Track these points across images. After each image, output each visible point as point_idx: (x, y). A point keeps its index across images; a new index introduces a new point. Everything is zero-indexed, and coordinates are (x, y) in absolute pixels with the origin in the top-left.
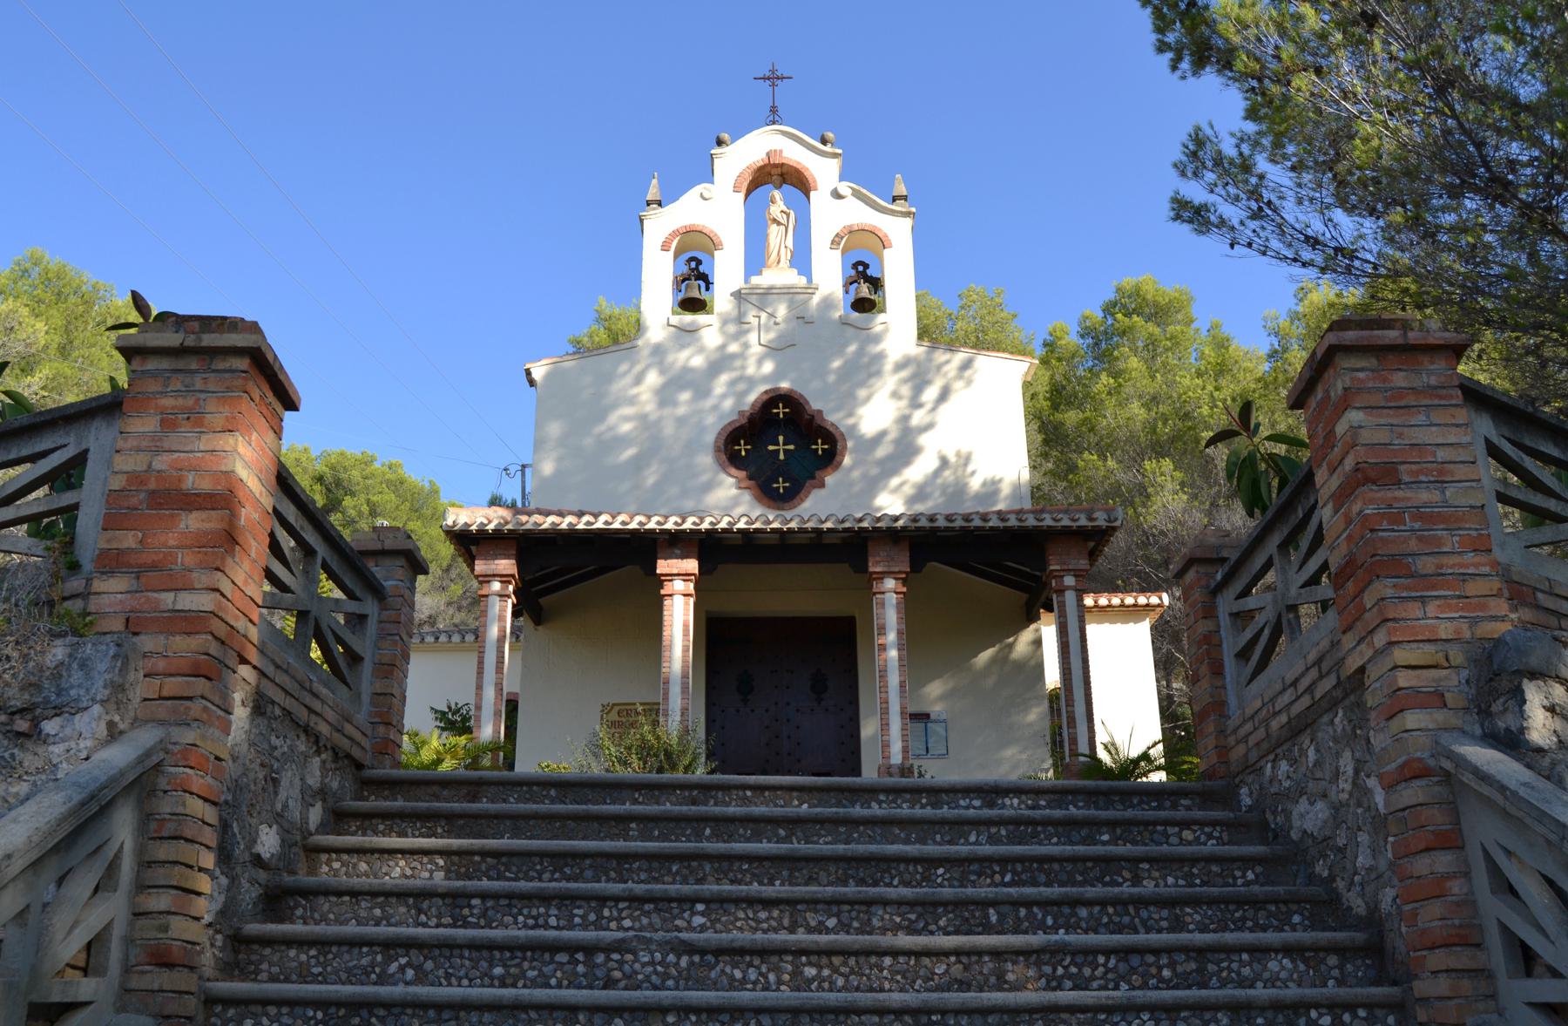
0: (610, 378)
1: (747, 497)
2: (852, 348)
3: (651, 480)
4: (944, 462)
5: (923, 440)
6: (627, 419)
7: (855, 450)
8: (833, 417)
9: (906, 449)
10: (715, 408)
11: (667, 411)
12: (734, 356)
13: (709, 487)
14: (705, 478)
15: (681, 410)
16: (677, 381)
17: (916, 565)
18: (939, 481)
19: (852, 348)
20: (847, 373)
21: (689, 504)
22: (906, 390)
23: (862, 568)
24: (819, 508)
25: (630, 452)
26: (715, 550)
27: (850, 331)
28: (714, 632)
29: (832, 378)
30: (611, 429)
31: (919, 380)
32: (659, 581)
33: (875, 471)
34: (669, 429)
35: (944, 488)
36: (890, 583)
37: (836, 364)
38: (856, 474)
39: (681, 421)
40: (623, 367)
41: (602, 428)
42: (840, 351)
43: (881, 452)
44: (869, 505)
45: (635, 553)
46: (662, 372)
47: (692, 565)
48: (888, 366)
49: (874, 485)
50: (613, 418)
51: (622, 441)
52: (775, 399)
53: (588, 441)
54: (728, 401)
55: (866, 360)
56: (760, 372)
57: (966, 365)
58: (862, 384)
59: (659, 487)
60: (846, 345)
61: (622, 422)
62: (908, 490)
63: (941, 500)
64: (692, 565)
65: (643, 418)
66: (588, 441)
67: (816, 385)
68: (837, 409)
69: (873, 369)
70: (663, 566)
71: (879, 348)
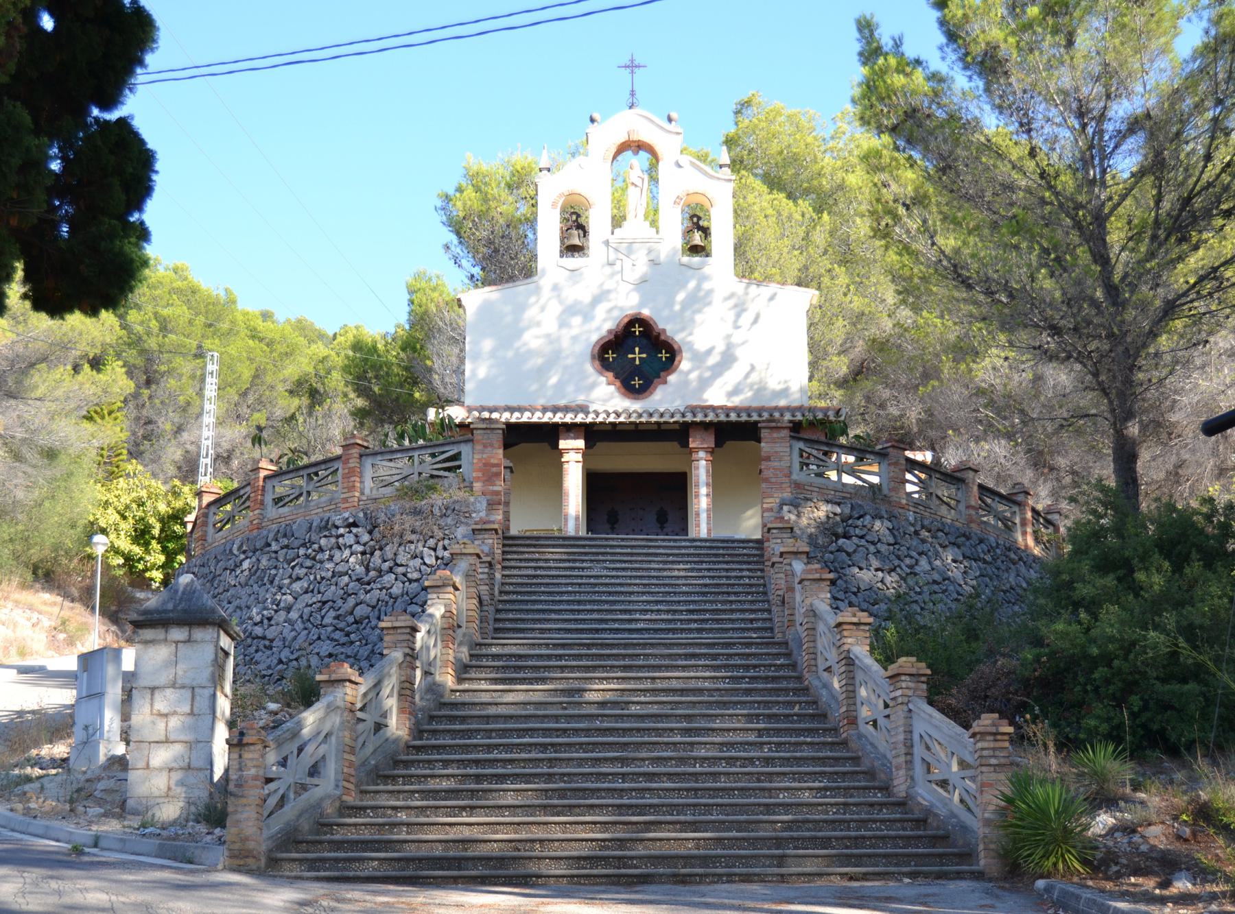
0: (522, 308)
1: (617, 394)
2: (692, 284)
3: (553, 380)
4: (753, 368)
5: (738, 352)
6: (537, 337)
7: (691, 360)
8: (678, 338)
9: (728, 359)
10: (598, 329)
11: (564, 331)
12: (609, 292)
13: (593, 386)
14: (591, 380)
15: (575, 332)
16: (571, 310)
17: (719, 443)
18: (749, 381)
19: (692, 284)
20: (685, 305)
21: (581, 399)
22: (731, 315)
23: (685, 444)
24: (665, 401)
25: (540, 361)
26: (594, 434)
27: (690, 272)
28: (594, 483)
29: (677, 307)
30: (525, 344)
31: (740, 309)
32: (560, 453)
33: (707, 374)
34: (565, 343)
35: (751, 386)
36: (702, 454)
37: (681, 296)
38: (693, 376)
39: (575, 339)
40: (533, 299)
41: (517, 344)
42: (683, 285)
43: (713, 360)
44: (701, 399)
45: (548, 435)
46: (561, 302)
47: (581, 443)
48: (717, 298)
49: (704, 383)
50: (527, 336)
51: (531, 353)
52: (637, 320)
53: (510, 354)
54: (603, 324)
55: (702, 294)
56: (626, 302)
57: (772, 298)
58: (699, 311)
59: (559, 386)
60: (687, 282)
61: (532, 340)
62: (729, 388)
63: (750, 394)
64: (581, 443)
65: (548, 336)
66: (510, 354)
67: (666, 313)
68: (683, 329)
69: (708, 300)
70: (563, 444)
71: (706, 286)
